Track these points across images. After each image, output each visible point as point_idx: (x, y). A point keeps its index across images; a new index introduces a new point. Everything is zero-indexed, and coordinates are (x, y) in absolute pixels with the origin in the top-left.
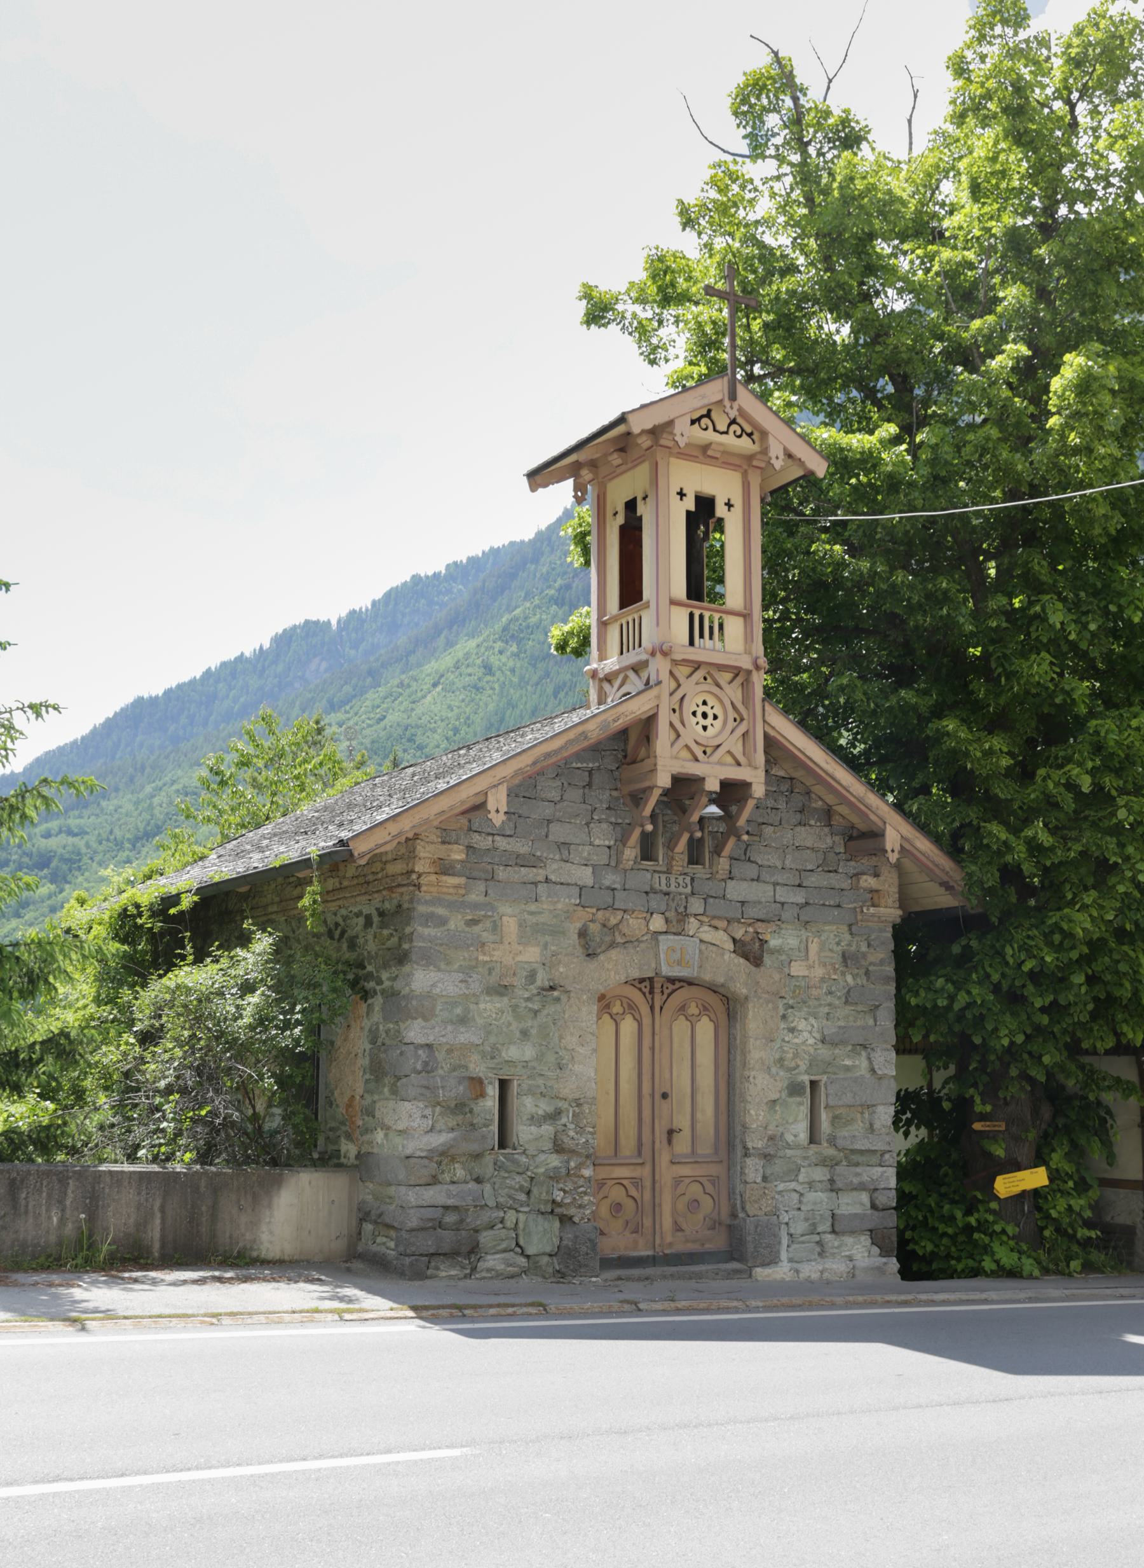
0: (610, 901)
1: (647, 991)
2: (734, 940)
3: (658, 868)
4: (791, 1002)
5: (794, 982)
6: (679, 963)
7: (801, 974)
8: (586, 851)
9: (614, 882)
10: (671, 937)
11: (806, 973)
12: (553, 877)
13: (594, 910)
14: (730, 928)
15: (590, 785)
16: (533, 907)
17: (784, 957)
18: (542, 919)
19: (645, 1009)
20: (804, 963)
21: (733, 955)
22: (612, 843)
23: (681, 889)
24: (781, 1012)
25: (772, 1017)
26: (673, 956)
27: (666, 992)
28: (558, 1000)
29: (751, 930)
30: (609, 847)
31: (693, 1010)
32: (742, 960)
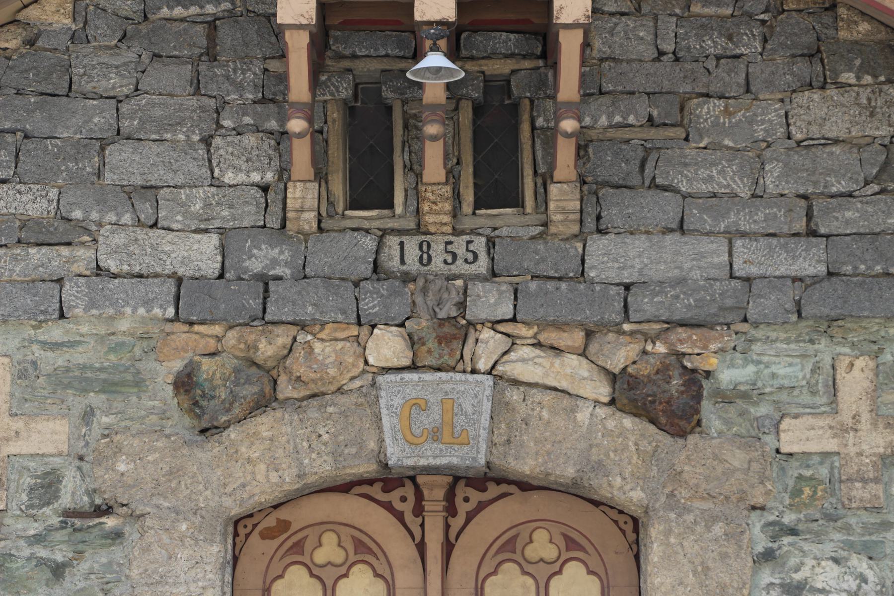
0: (255, 304)
1: (406, 508)
2: (613, 378)
3: (391, 224)
4: (789, 518)
5: (794, 470)
6: (435, 435)
7: (812, 447)
8: (198, 200)
9: (275, 262)
10: (428, 376)
11: (832, 445)
12: (112, 265)
13: (217, 329)
14: (593, 348)
15: (211, 54)
16: (56, 332)
17: (763, 410)
18: (78, 357)
19: (399, 548)
20: (828, 421)
21: (609, 410)
22: (270, 176)
23: (460, 267)
24: (762, 544)
25: (724, 556)
26: (423, 418)
27: (463, 508)
28: (117, 535)
29: (661, 348)
30: (265, 189)
31: (543, 547)
32: (628, 422)
